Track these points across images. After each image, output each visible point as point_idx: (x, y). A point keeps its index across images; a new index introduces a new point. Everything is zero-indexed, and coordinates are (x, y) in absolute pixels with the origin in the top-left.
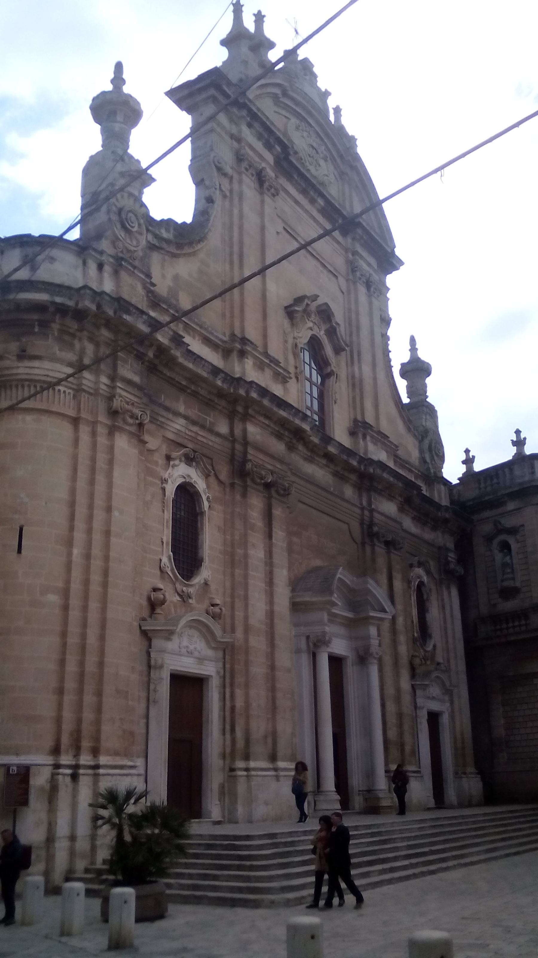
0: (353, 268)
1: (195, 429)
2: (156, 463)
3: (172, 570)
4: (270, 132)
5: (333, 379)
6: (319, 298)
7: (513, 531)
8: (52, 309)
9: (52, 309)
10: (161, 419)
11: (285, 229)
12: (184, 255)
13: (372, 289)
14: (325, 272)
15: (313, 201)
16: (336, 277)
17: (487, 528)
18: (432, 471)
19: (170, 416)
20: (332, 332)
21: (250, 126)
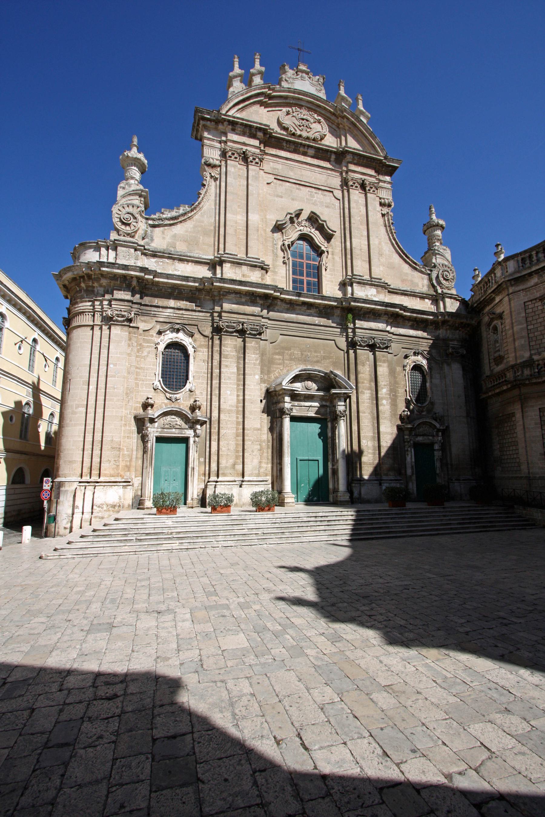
1: (181, 312)
2: (152, 336)
3: (162, 387)
4: (251, 127)
5: (324, 256)
6: (303, 212)
7: (500, 316)
8: (78, 278)
9: (78, 278)
10: (153, 313)
11: (275, 178)
12: (181, 222)
13: (367, 189)
14: (320, 192)
15: (305, 154)
16: (332, 192)
17: (486, 319)
18: (440, 291)
19: (161, 310)
20: (321, 229)
21: (233, 130)
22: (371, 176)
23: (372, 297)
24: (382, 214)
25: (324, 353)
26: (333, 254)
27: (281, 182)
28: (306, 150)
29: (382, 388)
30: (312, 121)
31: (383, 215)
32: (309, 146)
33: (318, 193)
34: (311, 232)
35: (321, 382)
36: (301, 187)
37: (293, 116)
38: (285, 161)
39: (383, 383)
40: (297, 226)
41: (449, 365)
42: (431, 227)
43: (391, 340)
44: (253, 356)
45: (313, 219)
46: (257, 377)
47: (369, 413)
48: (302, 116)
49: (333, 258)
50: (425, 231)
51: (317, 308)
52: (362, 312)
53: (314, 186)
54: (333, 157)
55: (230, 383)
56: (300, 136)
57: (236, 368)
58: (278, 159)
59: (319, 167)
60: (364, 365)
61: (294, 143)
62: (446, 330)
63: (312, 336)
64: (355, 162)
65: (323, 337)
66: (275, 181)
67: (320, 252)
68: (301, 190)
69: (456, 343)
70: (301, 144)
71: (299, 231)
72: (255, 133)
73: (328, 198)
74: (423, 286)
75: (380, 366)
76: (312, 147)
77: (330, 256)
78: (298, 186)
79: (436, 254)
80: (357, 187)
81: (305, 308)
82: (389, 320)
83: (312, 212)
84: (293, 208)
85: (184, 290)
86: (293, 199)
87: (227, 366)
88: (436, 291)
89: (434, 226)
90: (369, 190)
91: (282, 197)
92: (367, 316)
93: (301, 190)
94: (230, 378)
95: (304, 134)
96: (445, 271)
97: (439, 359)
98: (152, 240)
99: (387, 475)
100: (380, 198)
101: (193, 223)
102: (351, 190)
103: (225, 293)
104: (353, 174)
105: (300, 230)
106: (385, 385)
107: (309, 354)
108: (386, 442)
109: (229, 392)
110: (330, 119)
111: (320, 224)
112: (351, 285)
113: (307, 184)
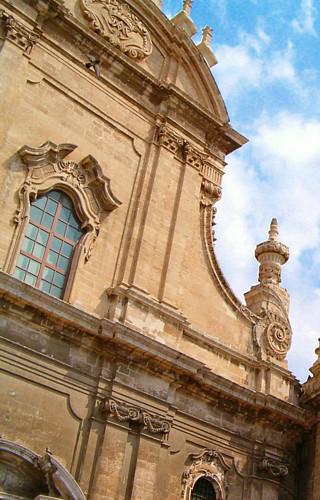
0: (157, 136)
5: (90, 235)
11: (44, 79)
13: (188, 157)
14: (113, 131)
18: (264, 357)
20: (99, 189)
22: (198, 142)
23: (156, 335)
24: (201, 204)
25: (41, 415)
26: (105, 238)
27: (53, 90)
28: (110, 61)
30: (132, 28)
31: (202, 206)
32: (116, 59)
34: (77, 188)
35: (19, 475)
36: (84, 111)
37: (105, 8)
38: (71, 62)
40: (57, 169)
42: (269, 251)
43: (171, 422)
45: (89, 167)
49: (105, 246)
50: (259, 254)
51: (52, 323)
52: (131, 357)
53: (105, 118)
56: (107, 39)
58: (59, 54)
59: (122, 94)
61: (94, 43)
62: (264, 426)
63: (27, 375)
64: (180, 111)
65: (47, 383)
66: (44, 83)
67: (85, 225)
68: (82, 115)
70: (105, 50)
71: (58, 177)
73: (123, 145)
74: (240, 341)
76: (121, 62)
77: (99, 239)
78: (79, 107)
79: (269, 296)
80: (173, 148)
81: (30, 318)
82: (175, 384)
83: (90, 157)
84: (62, 137)
86: (64, 124)
88: (259, 358)
89: (274, 251)
90: (191, 161)
91: (46, 112)
92: (140, 366)
93: (82, 115)
96: (278, 327)
100: (204, 180)
102: (162, 149)
104: (172, 127)
105: (61, 178)
107: (10, 409)
111: (98, 180)
112: (126, 300)
113: (95, 111)
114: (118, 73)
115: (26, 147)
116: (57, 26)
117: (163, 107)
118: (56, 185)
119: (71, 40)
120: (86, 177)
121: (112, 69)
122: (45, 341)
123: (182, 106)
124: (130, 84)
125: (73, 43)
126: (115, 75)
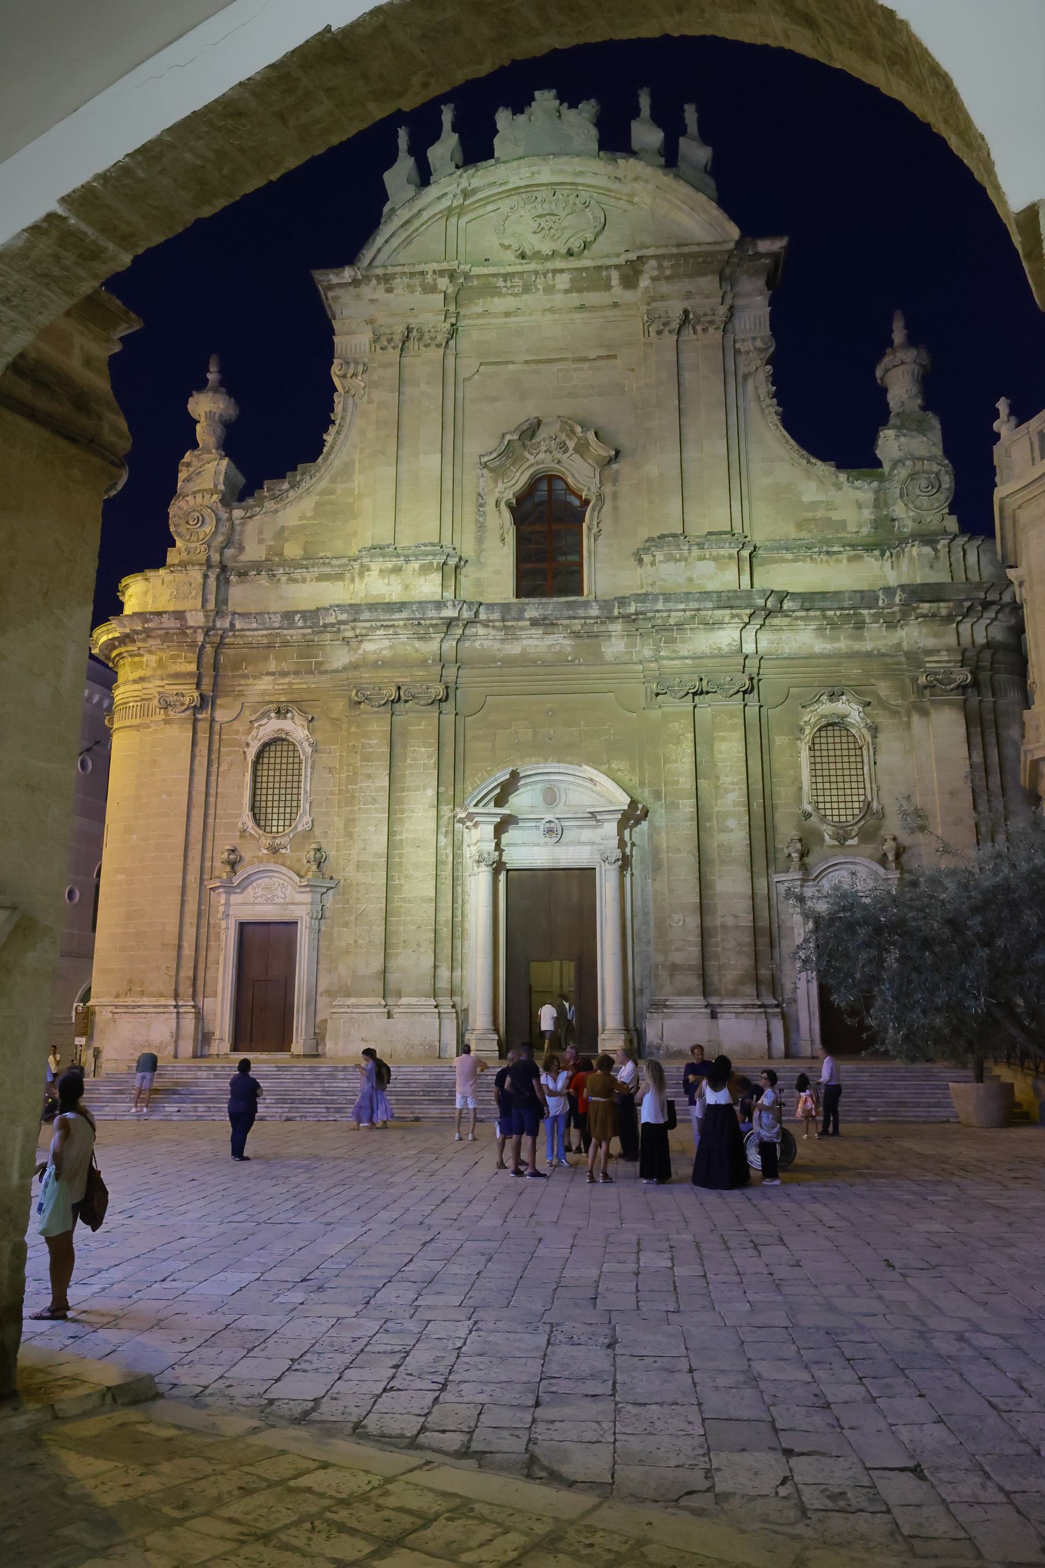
2: (237, 732)
29: (727, 791)
32: (555, 271)
33: (582, 369)
39: (729, 780)
40: (529, 456)
41: (924, 713)
44: (423, 750)
46: (431, 793)
47: (689, 852)
48: (540, 211)
54: (615, 275)
55: (376, 810)
57: (387, 778)
60: (678, 743)
64: (668, 272)
69: (947, 658)
71: (531, 465)
72: (432, 282)
75: (723, 739)
76: (562, 271)
78: (533, 366)
85: (291, 636)
87: (369, 776)
94: (374, 800)
95: (546, 248)
97: (900, 702)
98: (241, 549)
99: (734, 994)
101: (316, 498)
103: (364, 632)
105: (537, 463)
106: (733, 784)
107: (551, 731)
108: (735, 917)
109: (372, 829)
110: (611, 191)
114: (567, 286)
115: (481, 456)
116: (471, 288)
117: (644, 282)
118: (532, 477)
119: (496, 292)
120: (568, 442)
121: (558, 287)
122: (569, 649)
123: (666, 264)
124: (588, 289)
125: (499, 294)
126: (567, 291)
